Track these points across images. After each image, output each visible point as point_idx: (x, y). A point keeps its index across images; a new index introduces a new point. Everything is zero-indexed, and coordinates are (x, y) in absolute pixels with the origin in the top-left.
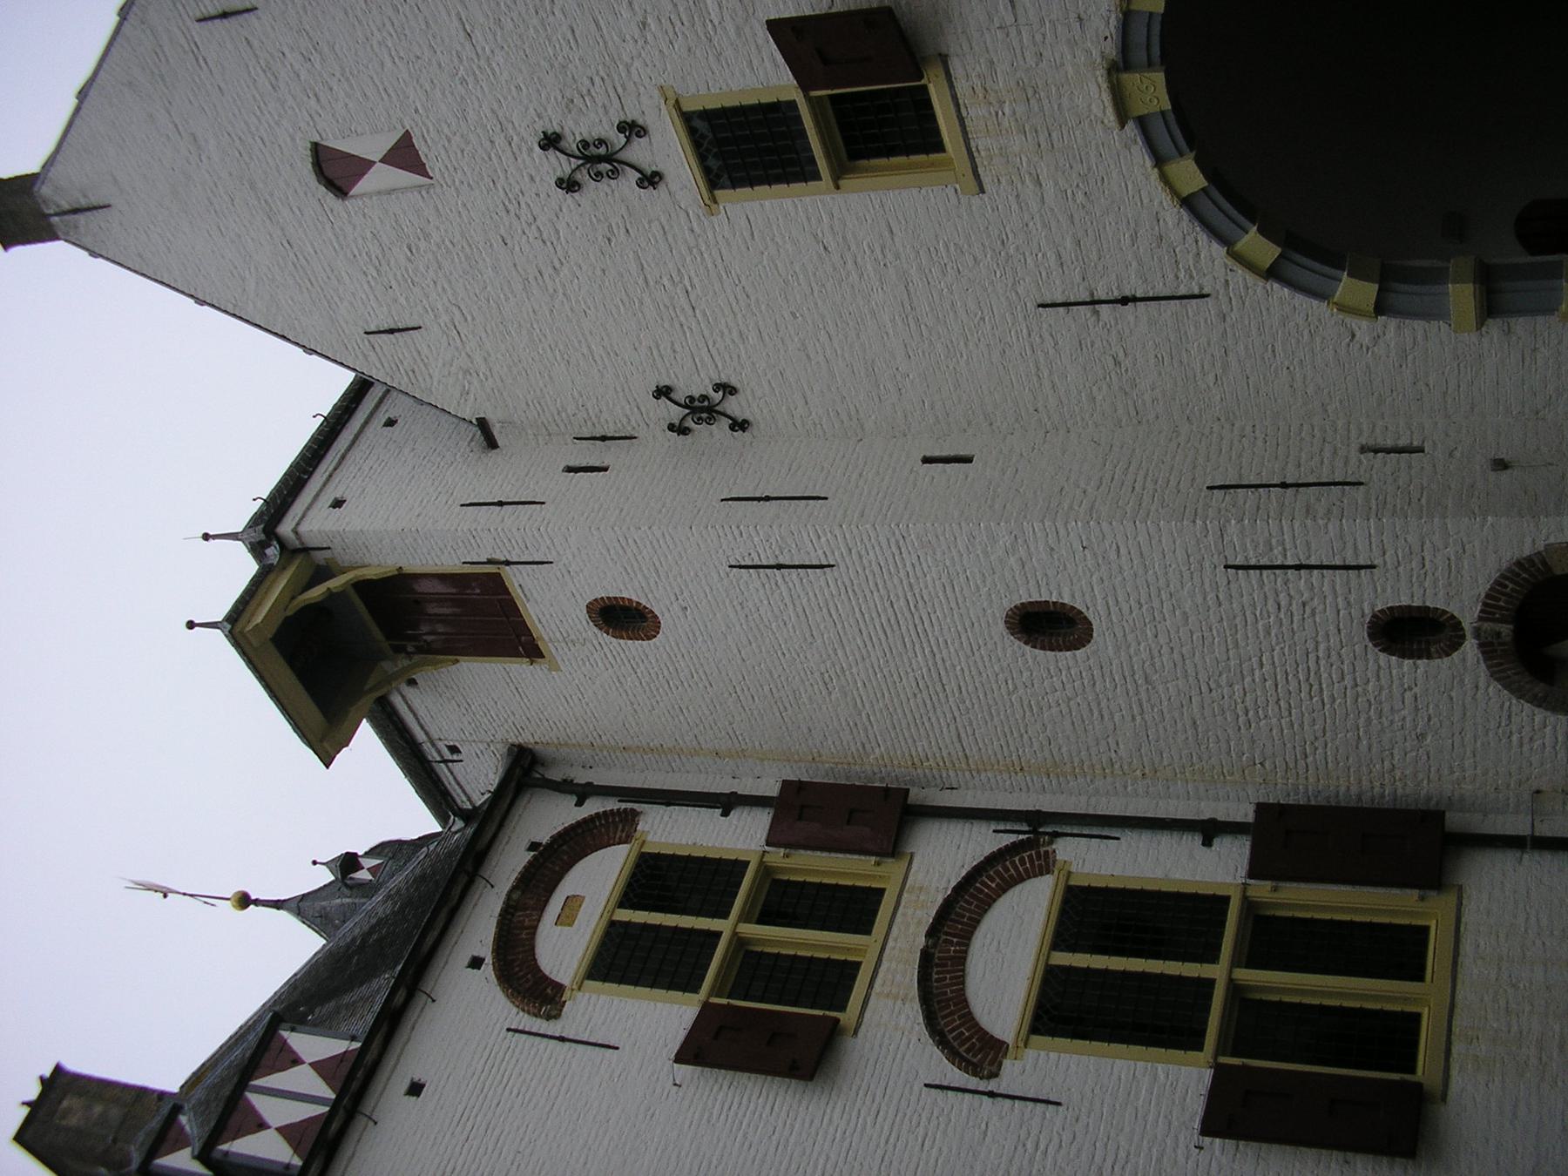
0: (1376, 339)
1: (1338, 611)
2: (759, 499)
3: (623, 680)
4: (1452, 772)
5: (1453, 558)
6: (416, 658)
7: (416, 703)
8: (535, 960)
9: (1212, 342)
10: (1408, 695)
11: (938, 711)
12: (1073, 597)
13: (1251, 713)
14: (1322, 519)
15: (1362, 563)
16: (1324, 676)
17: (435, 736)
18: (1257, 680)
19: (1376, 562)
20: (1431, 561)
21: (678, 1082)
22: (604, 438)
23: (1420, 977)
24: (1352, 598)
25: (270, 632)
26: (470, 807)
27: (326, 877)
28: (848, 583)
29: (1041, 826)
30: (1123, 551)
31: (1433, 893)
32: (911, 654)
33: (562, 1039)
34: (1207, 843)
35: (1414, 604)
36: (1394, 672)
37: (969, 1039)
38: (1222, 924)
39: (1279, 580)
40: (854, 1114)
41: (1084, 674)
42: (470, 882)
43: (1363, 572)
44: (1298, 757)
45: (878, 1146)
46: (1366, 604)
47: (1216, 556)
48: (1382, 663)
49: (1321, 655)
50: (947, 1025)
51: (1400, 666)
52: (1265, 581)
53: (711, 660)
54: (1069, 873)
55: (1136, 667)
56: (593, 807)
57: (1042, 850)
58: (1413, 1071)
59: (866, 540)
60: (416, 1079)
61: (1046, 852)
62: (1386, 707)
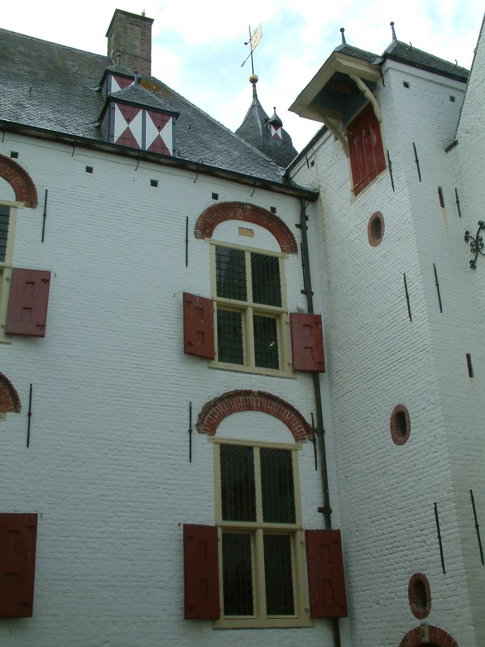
1: (424, 558)
2: (437, 281)
3: (351, 234)
5: (453, 611)
6: (346, 138)
7: (328, 142)
8: (221, 222)
10: (394, 594)
11: (359, 380)
12: (414, 434)
13: (377, 523)
14: (462, 546)
15: (446, 567)
17: (317, 154)
18: (391, 524)
19: (447, 574)
21: (176, 295)
22: (458, 202)
23: (269, 612)
24: (430, 564)
25: (340, 70)
26: (291, 176)
27: (270, 114)
28: (405, 329)
29: (317, 434)
30: (436, 454)
31: (309, 615)
32: (381, 363)
33: (187, 242)
34: (320, 510)
35: (431, 594)
36: (402, 587)
37: (214, 418)
38: (282, 521)
39: (433, 529)
40: (173, 374)
41: (383, 444)
42: (252, 186)
43: (442, 568)
45: (161, 386)
47: (439, 498)
48: (405, 581)
49: (405, 552)
50: (219, 407)
53: (365, 273)
54: (297, 450)
55: (389, 467)
56: (296, 233)
57: (306, 436)
58: (226, 613)
59: (424, 334)
60: (158, 183)
61: (305, 438)
62: (387, 585)
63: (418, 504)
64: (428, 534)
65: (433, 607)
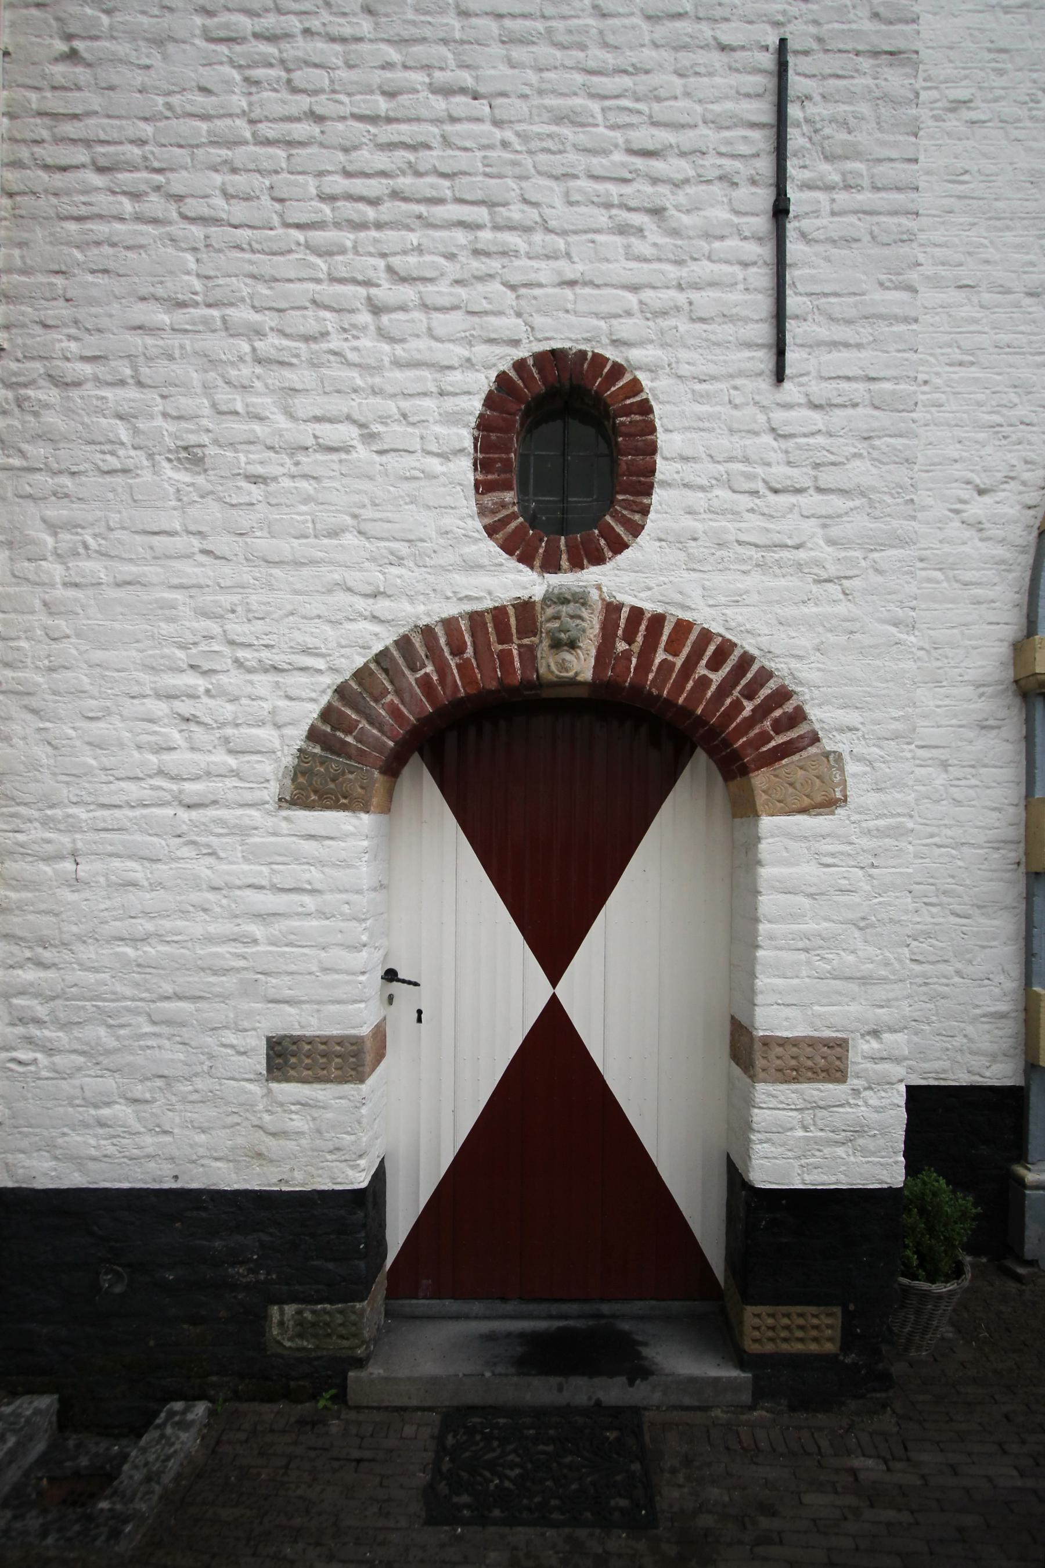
0: (978, 526)
1: (634, 288)
4: (53, 528)
5: (802, 555)
9: (989, 267)
15: (790, 356)
16: (414, 238)
18: (388, 74)
19: (787, 385)
20: (791, 509)
36: (427, 403)
39: (737, 164)
44: (101, 149)
46: (659, 353)
47: (812, 29)
51: (451, 418)
52: (727, 134)
63: (637, 20)
64: (687, 181)
65: (653, 523)
